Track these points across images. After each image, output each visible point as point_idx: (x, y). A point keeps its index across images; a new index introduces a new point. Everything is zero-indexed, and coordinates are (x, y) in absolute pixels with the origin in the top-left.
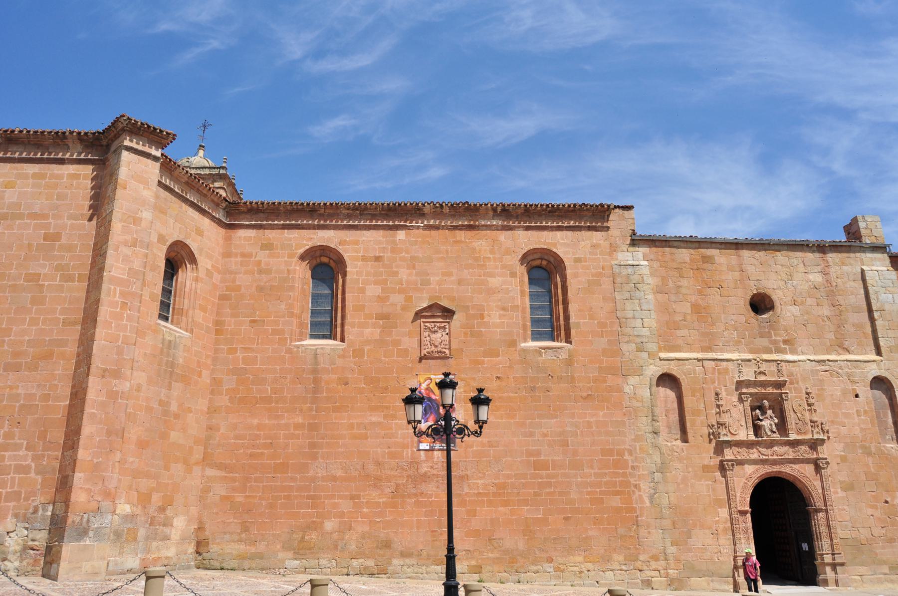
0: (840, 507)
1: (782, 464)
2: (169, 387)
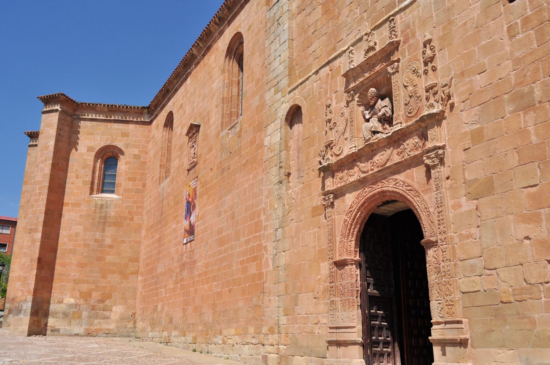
0: (464, 232)
1: (384, 179)
2: (103, 230)
